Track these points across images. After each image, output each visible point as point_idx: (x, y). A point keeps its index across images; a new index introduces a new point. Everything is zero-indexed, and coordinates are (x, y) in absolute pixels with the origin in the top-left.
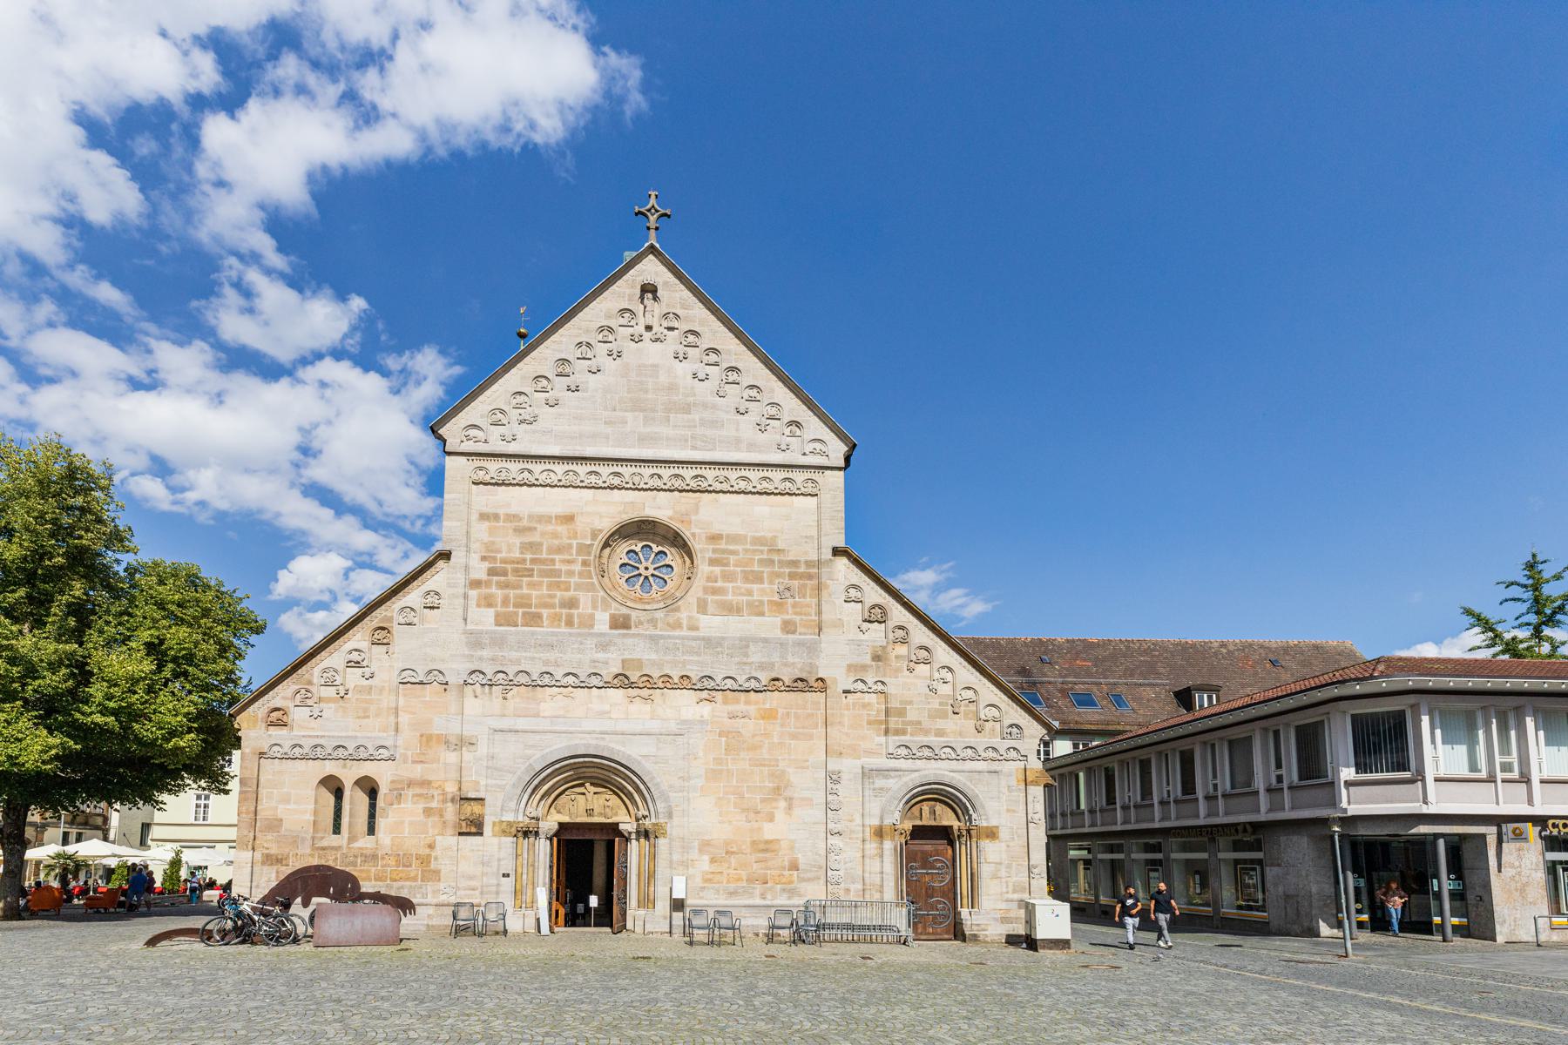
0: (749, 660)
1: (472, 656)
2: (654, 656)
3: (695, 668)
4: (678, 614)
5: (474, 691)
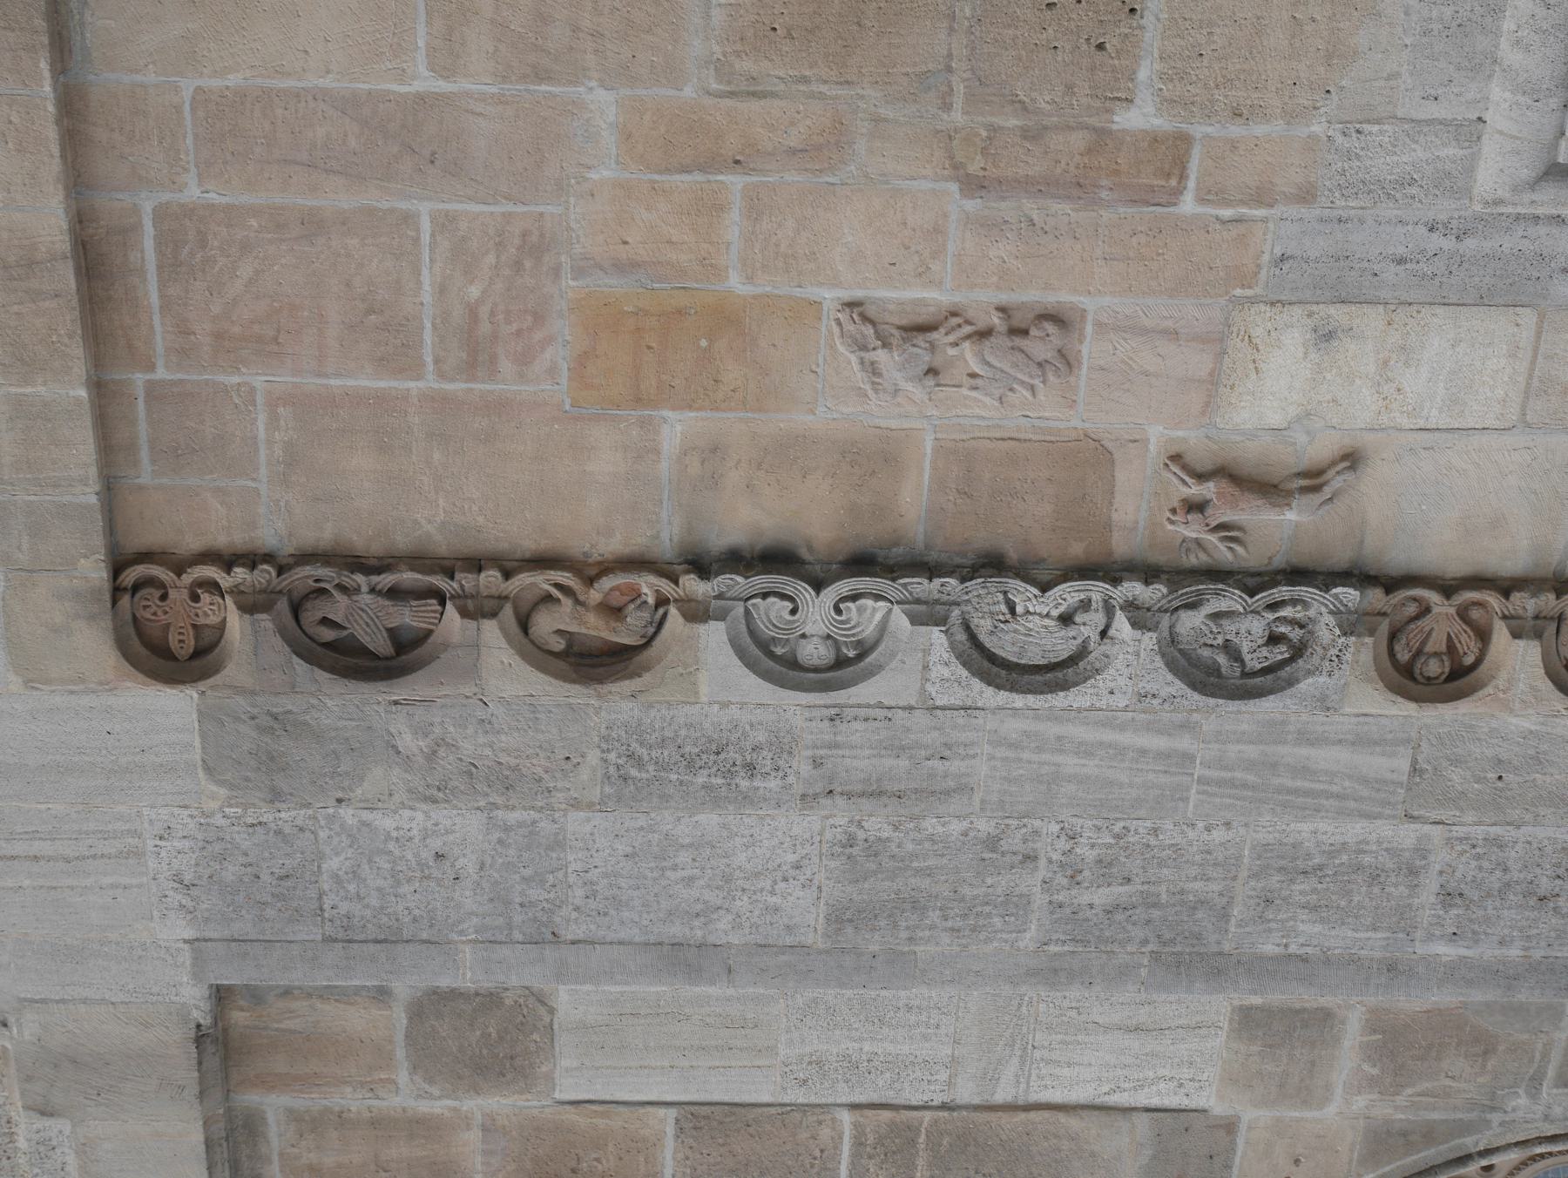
0: (840, 815)
3: (1325, 757)
4: (1395, 1110)
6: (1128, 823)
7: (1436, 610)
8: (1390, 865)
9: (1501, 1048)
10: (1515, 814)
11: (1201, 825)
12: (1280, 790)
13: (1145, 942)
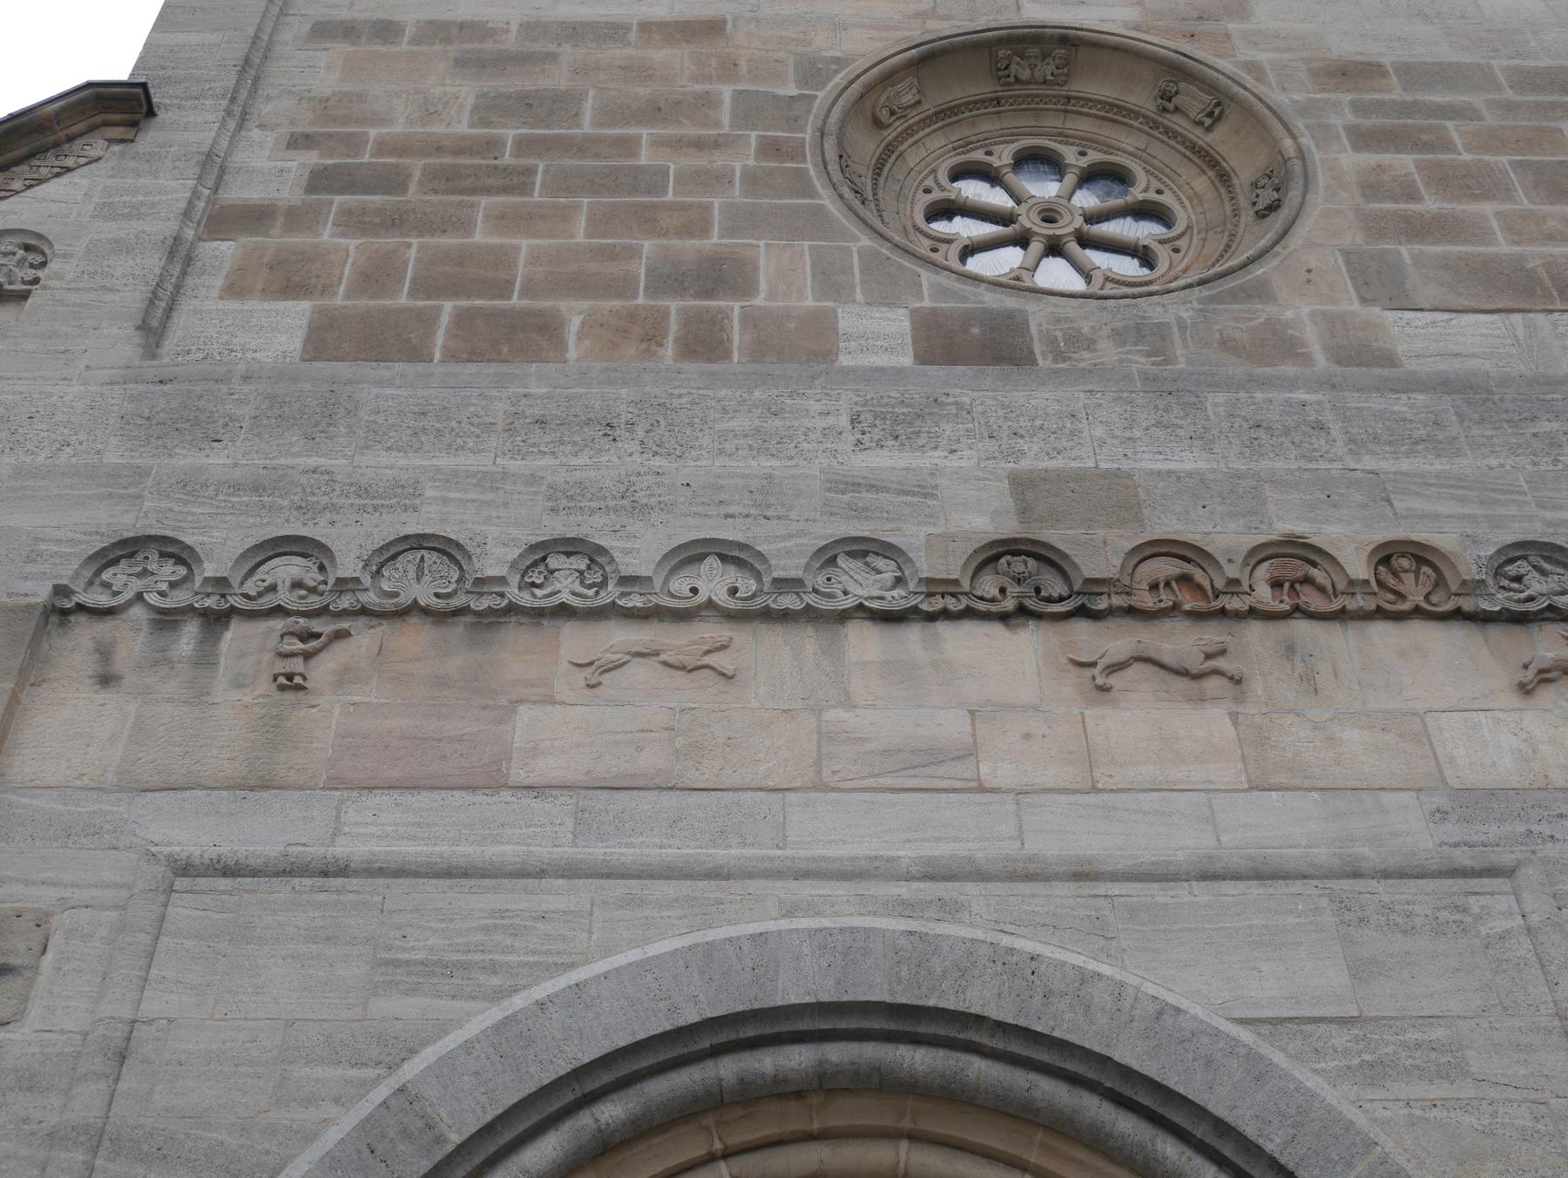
1: (140, 473)
2: (1189, 461)
5: (104, 652)
6: (1555, 468)
7: (1422, 598)
8: (1371, 446)
9: (1216, 345)
10: (1306, 475)
11: (1508, 468)
12: (1470, 488)
13: (1502, 400)
